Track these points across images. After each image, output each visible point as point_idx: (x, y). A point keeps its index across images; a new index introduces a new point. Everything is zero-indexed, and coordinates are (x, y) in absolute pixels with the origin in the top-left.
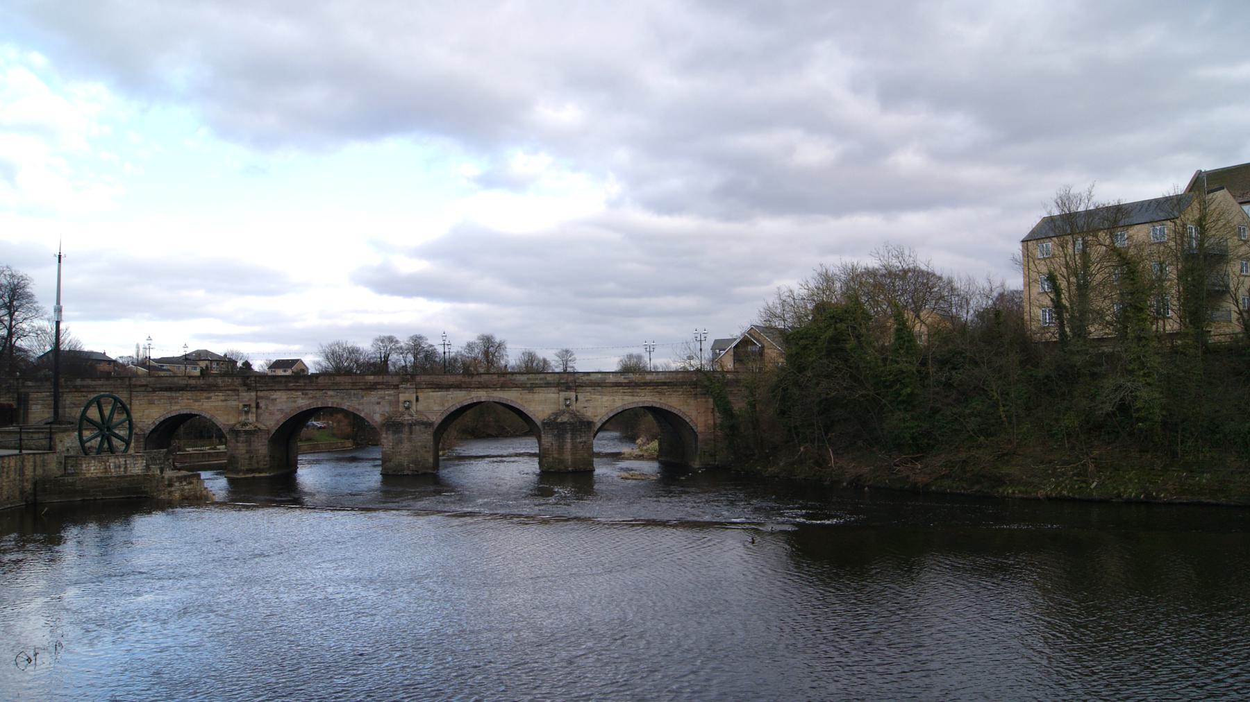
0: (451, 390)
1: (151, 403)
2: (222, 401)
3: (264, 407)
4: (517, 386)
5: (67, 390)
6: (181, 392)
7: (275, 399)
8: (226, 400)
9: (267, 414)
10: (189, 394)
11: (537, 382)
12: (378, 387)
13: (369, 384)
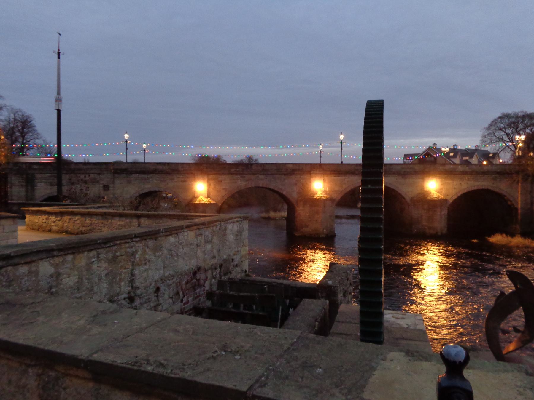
0: (348, 175)
1: (129, 182)
4: (394, 173)
6: (151, 175)
10: (158, 176)
11: (408, 170)
12: (297, 172)
13: (289, 170)
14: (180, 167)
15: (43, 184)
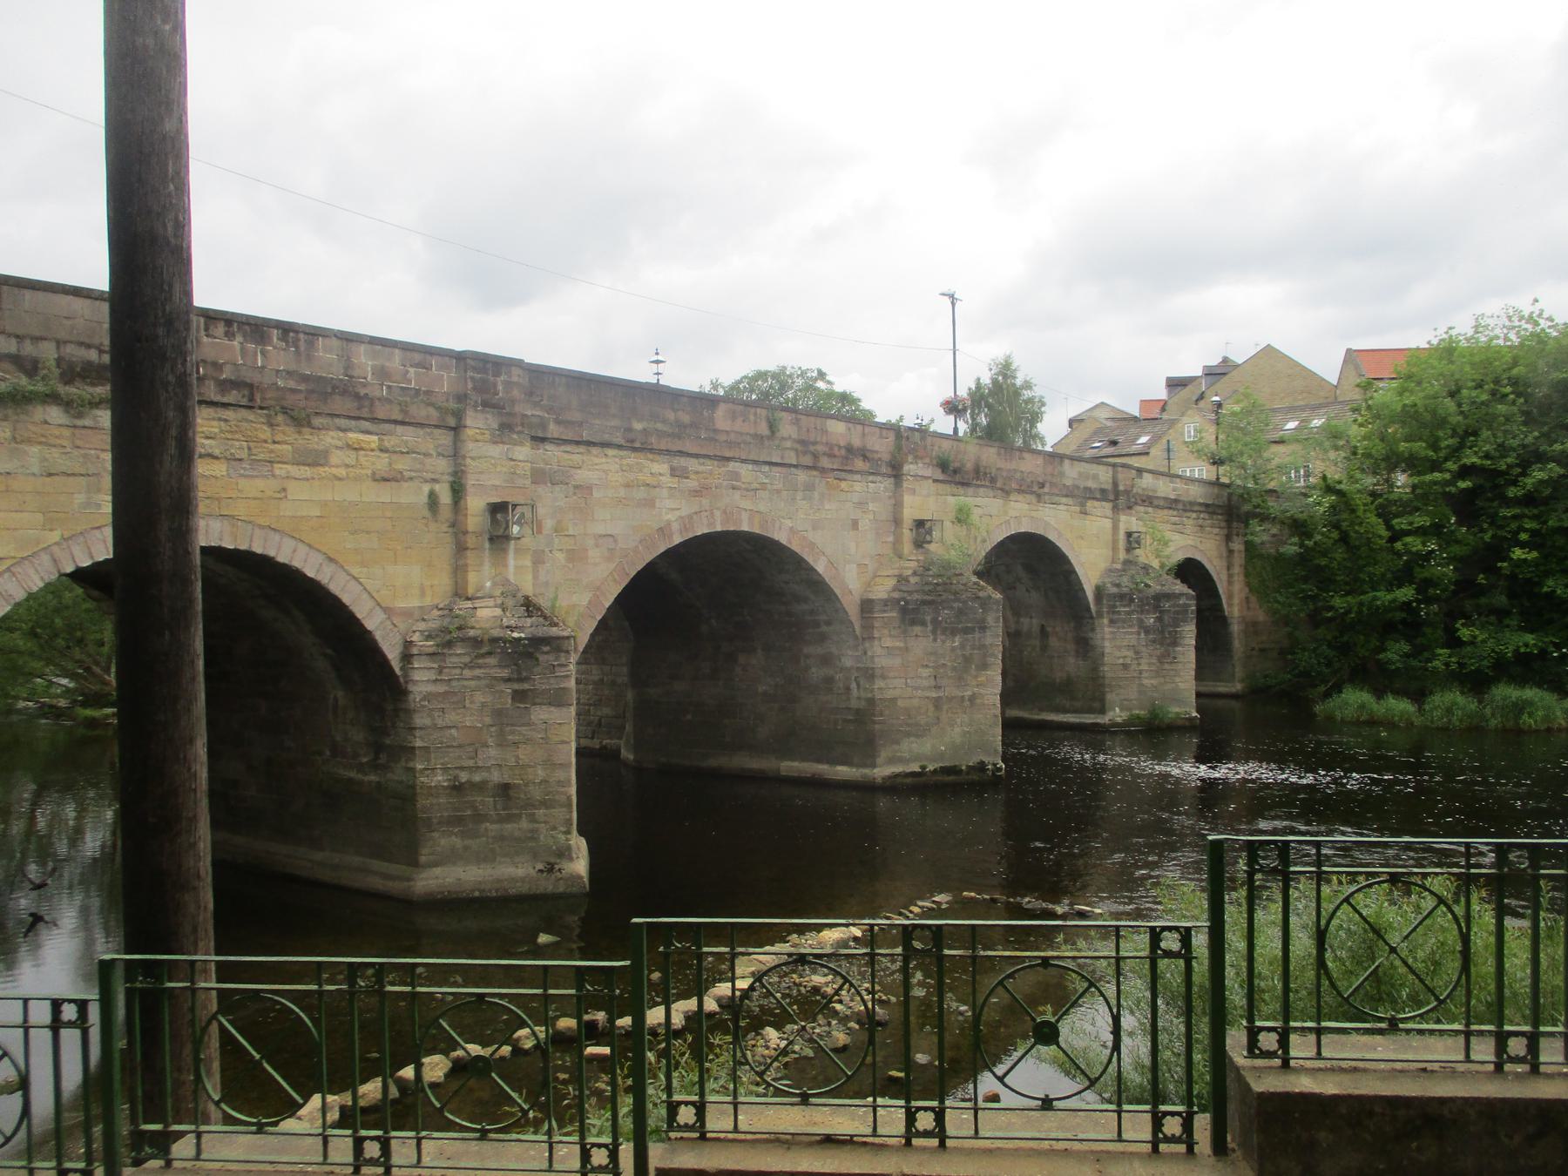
3: (548, 524)
7: (589, 488)
9: (560, 556)
14: (365, 362)
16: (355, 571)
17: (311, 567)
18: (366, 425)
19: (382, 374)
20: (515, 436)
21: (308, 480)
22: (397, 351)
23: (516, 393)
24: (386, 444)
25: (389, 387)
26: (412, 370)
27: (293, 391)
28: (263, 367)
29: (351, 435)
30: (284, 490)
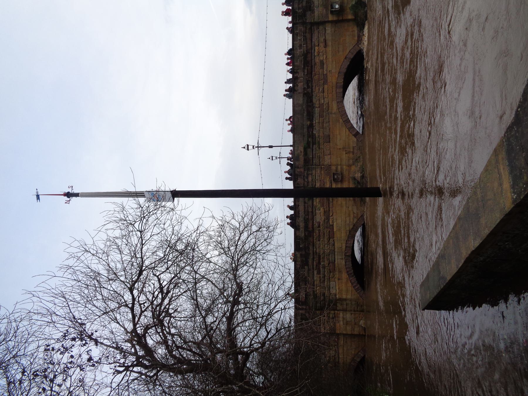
1: (328, 139)
2: (326, 46)
5: (311, 248)
6: (314, 100)
8: (325, 41)
10: (317, 91)
15: (332, 284)
16: (348, 51)
17: (347, 63)
18: (313, 51)
19: (300, 46)
20: (312, 6)
21: (327, 65)
22: (295, 43)
23: (300, 6)
24: (317, 45)
25: (304, 45)
26: (298, 38)
27: (307, 70)
28: (303, 78)
29: (316, 55)
30: (330, 71)
